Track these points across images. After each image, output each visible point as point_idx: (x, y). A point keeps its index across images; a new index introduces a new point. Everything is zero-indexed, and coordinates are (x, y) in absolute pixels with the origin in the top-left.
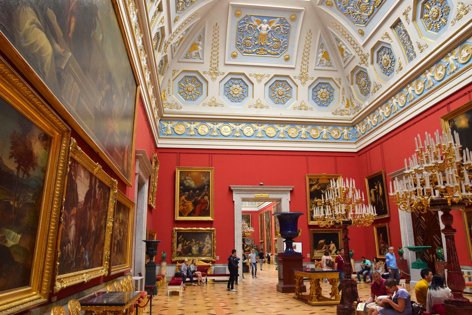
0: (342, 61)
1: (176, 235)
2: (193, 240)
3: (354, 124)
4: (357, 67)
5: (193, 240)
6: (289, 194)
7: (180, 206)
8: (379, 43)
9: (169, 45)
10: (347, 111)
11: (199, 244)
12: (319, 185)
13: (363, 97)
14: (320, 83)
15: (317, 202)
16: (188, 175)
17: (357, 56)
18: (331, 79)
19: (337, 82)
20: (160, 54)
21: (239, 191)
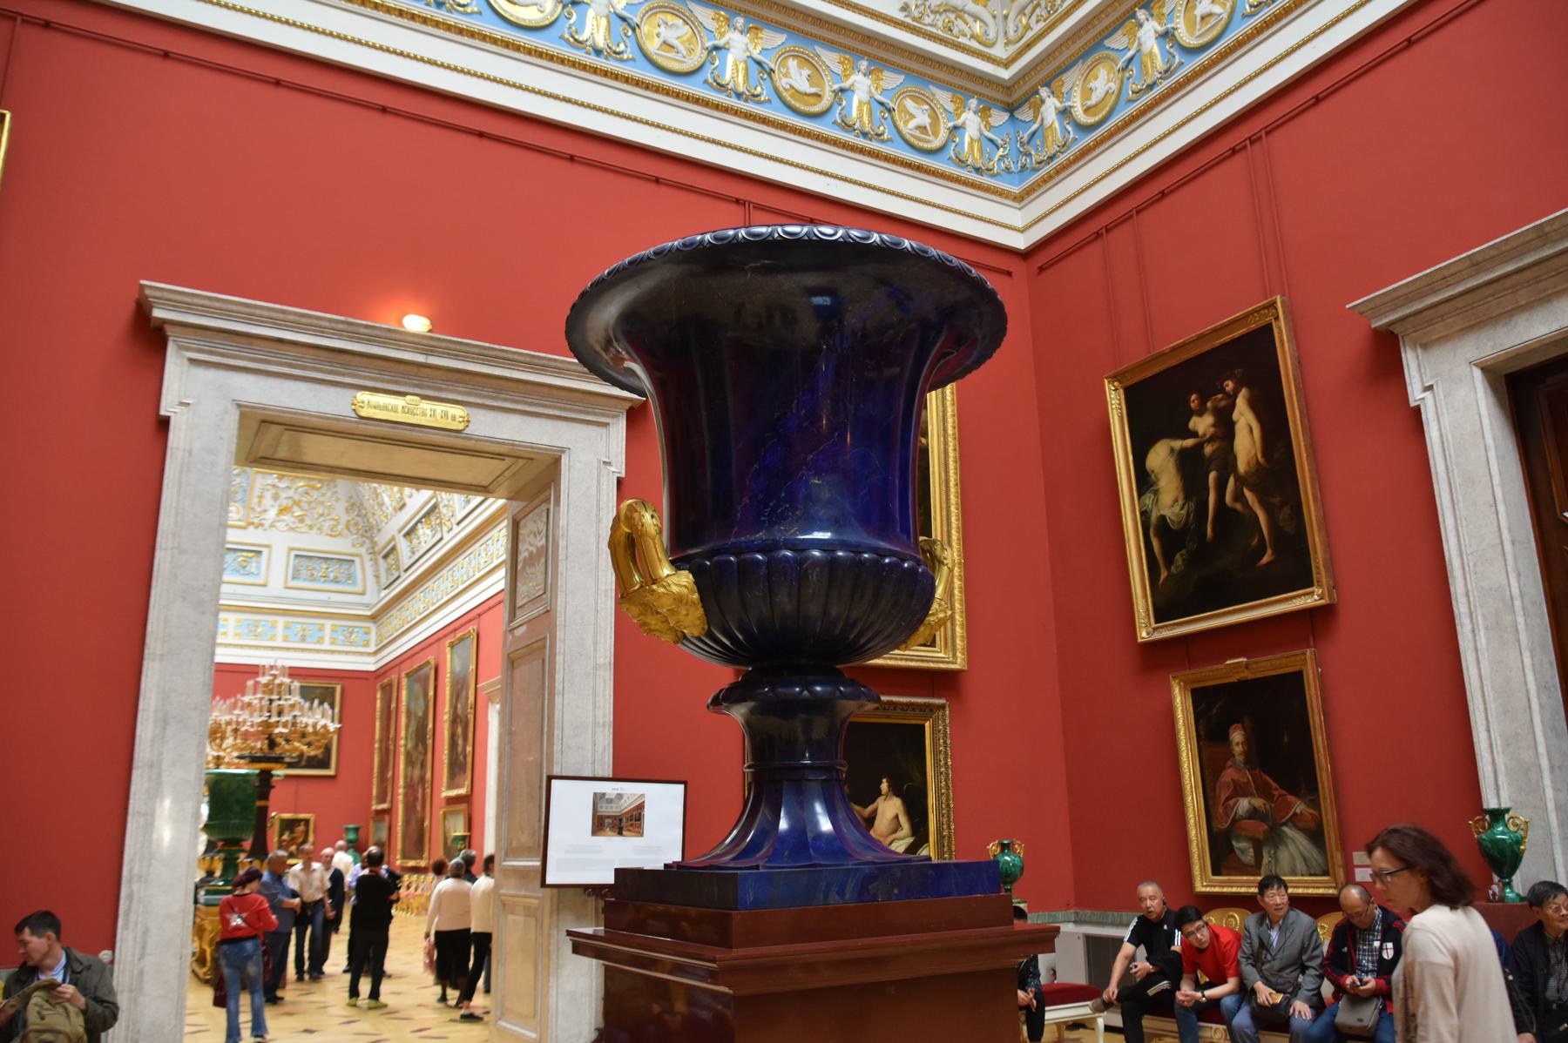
3: (1017, 94)
6: (619, 428)
10: (976, 18)
21: (230, 348)
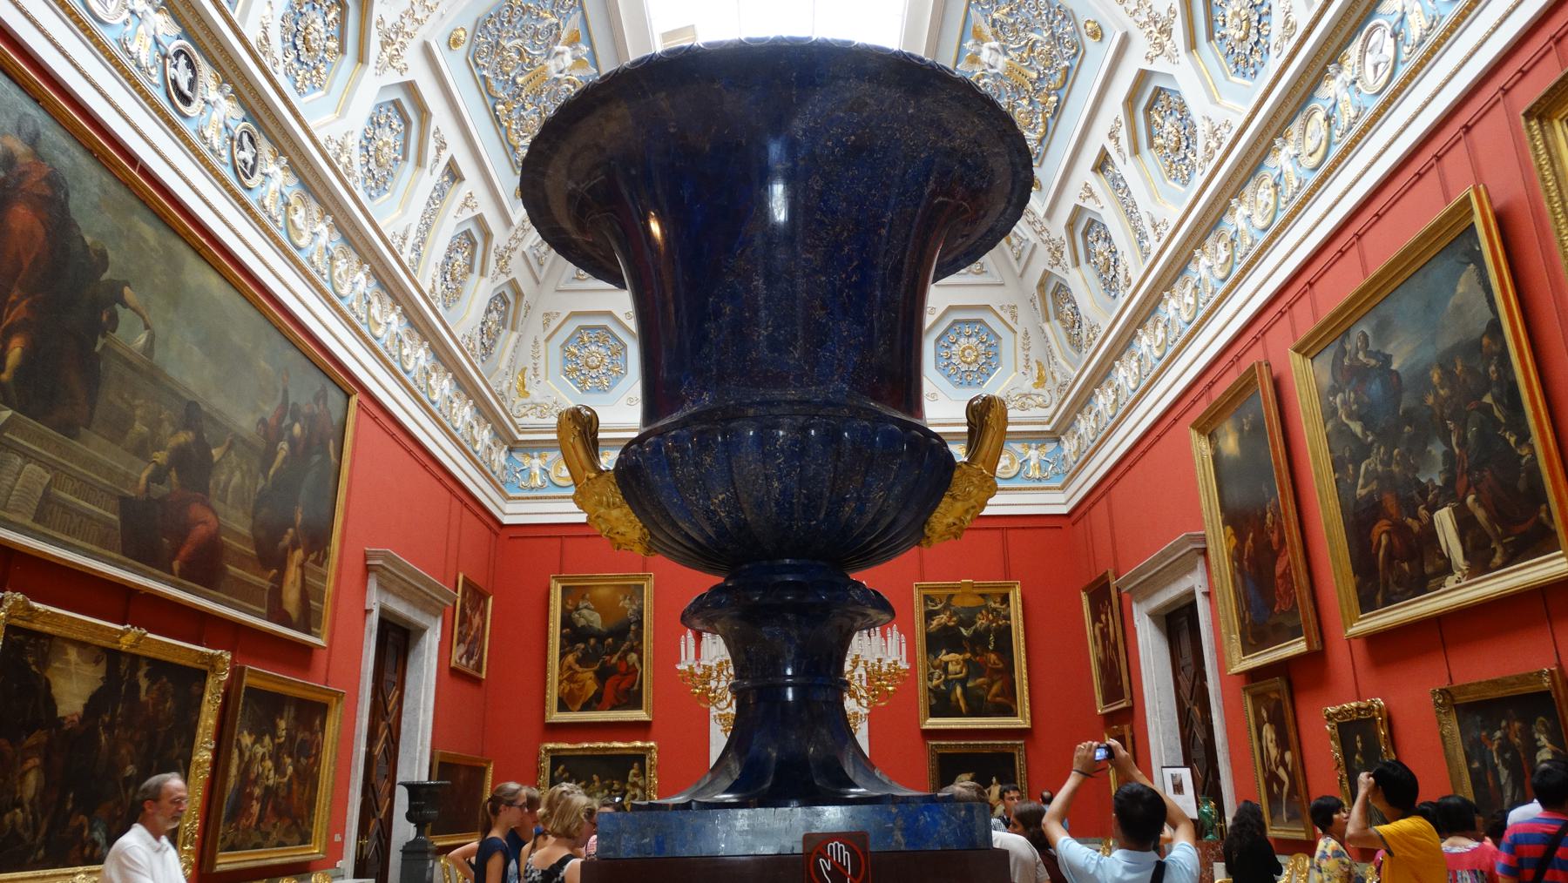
0: (1013, 260)
1: (546, 764)
2: (595, 777)
4: (1047, 275)
5: (595, 777)
7: (560, 683)
8: (1078, 211)
9: (517, 256)
11: (610, 788)
12: (955, 613)
13: (1074, 354)
14: (956, 322)
15: (947, 663)
16: (583, 597)
17: (1040, 244)
18: (987, 308)
19: (1007, 317)
20: (485, 282)
